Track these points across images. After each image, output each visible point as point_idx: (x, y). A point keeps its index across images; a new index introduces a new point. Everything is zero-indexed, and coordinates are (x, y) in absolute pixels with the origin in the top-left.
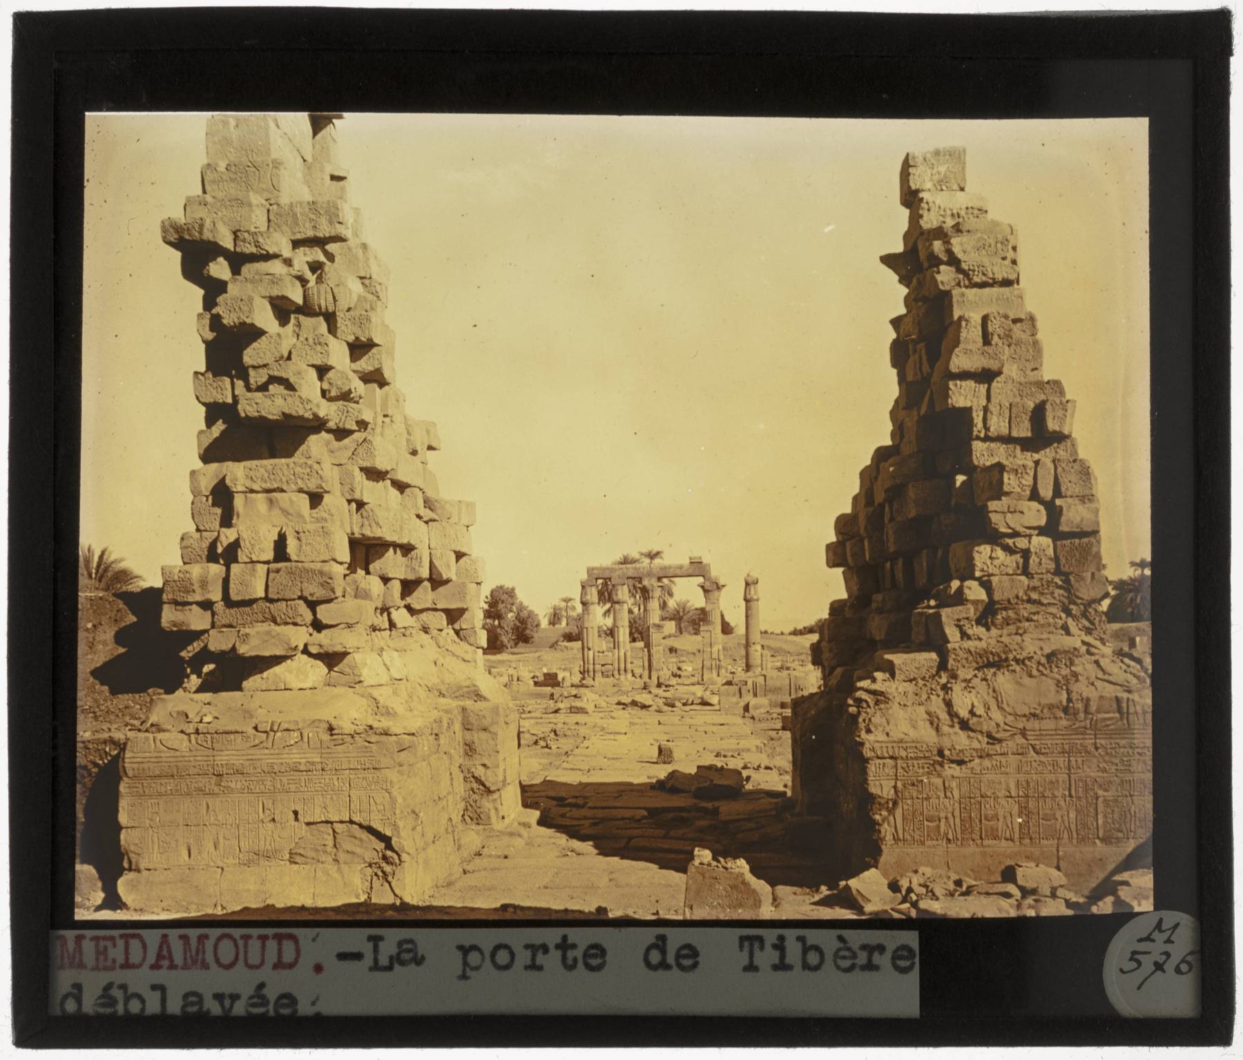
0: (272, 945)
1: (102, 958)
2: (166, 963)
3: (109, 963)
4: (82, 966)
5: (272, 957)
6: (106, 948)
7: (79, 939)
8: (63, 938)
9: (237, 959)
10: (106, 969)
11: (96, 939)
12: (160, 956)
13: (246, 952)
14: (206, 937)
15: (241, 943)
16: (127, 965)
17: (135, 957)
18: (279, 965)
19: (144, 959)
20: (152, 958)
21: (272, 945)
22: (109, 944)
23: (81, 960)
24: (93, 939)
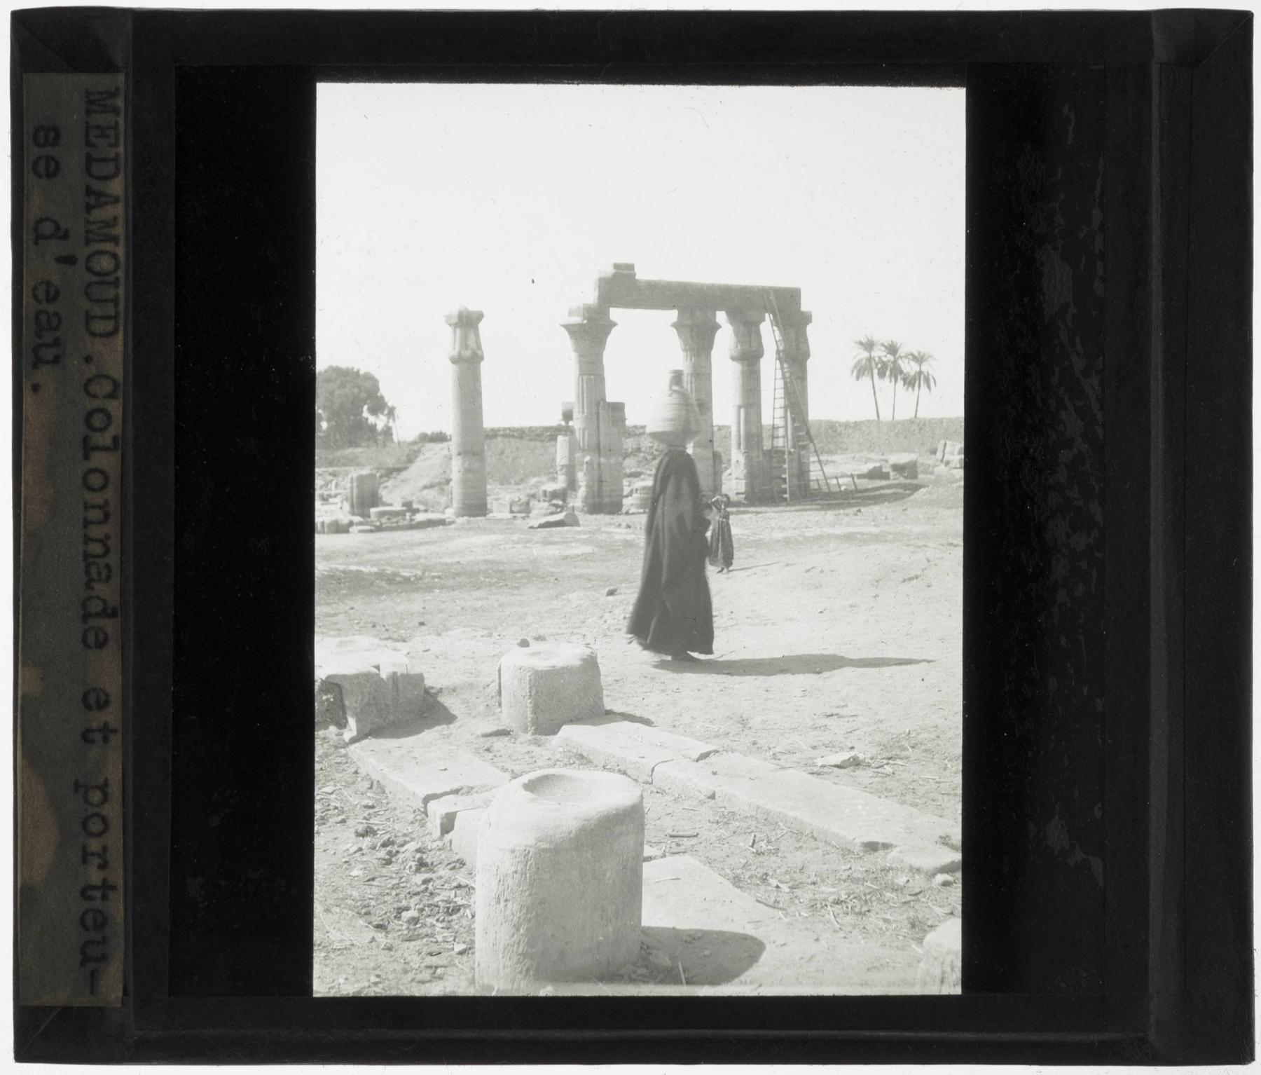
0: (110, 309)
1: (98, 132)
2: (92, 200)
3: (94, 140)
4: (88, 112)
5: (97, 310)
6: (108, 136)
7: (115, 111)
8: (114, 94)
9: (97, 274)
10: (87, 135)
11: (116, 127)
12: (99, 194)
13: (102, 283)
14: (117, 244)
15: (111, 278)
16: (90, 159)
17: (98, 169)
18: (89, 317)
19: (97, 178)
20: (96, 185)
21: (110, 309)
22: (112, 140)
23: (96, 112)
24: (117, 122)
